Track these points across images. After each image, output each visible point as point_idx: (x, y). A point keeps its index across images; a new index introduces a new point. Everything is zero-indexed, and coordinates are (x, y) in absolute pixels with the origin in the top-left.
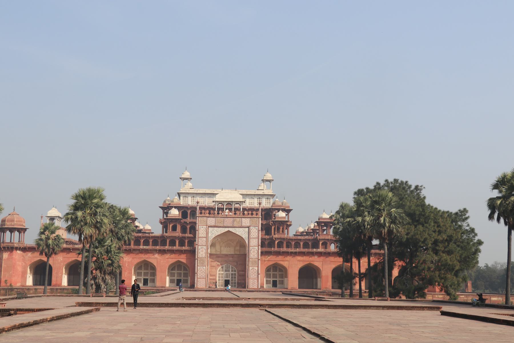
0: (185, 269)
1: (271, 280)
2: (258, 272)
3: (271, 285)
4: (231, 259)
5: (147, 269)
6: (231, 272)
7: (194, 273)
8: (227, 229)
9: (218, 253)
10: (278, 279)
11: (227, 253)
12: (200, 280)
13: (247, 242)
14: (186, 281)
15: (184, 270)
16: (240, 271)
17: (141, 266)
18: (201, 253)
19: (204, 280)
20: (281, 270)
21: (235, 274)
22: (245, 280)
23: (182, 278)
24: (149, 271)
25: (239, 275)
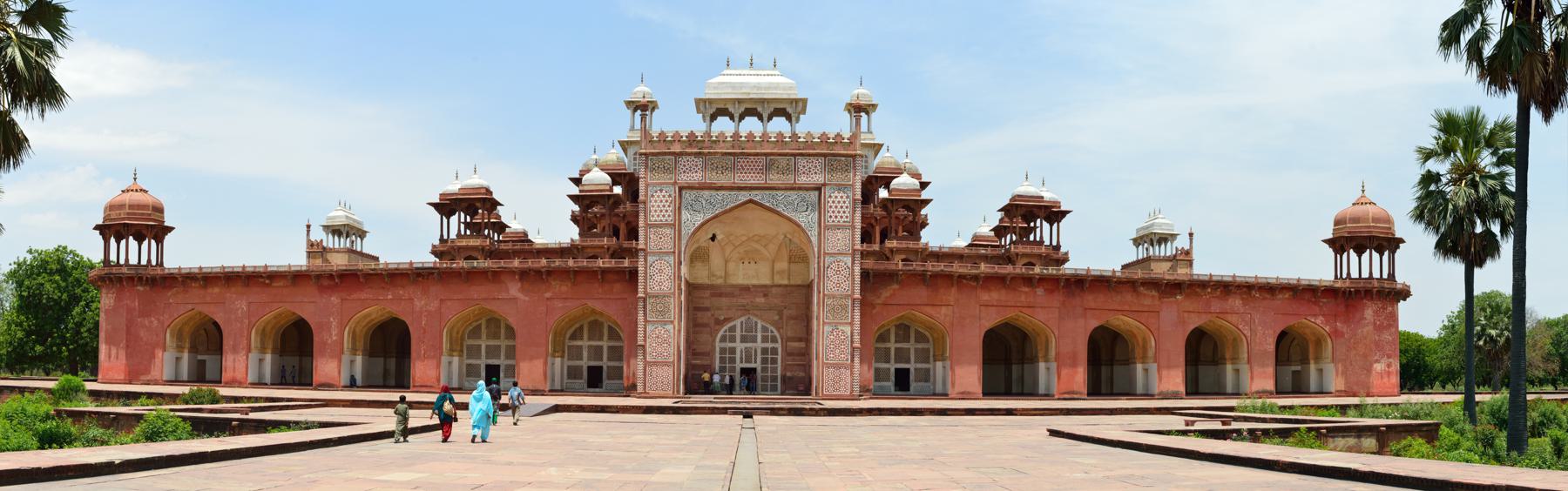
0: (614, 335)
1: (892, 366)
3: (890, 384)
4: (760, 300)
5: (496, 336)
6: (759, 345)
7: (636, 348)
8: (744, 196)
9: (720, 281)
10: (912, 366)
13: (814, 240)
15: (610, 338)
17: (479, 327)
18: (657, 278)
20: (921, 338)
21: (774, 351)
22: (807, 367)
23: (605, 363)
24: (503, 343)
25: (788, 353)
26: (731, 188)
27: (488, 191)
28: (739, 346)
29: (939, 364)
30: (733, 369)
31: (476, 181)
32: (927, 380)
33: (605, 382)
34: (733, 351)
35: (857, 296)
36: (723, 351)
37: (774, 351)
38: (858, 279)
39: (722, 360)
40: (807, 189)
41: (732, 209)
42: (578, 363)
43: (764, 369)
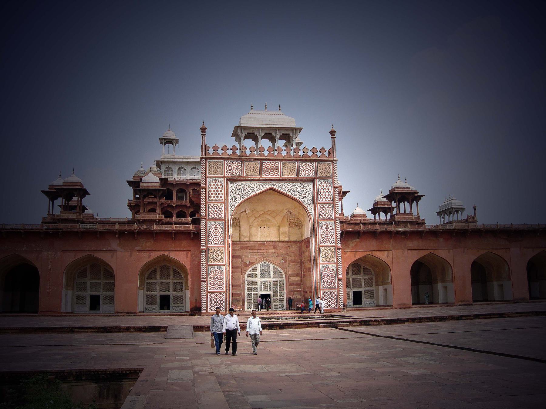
0: (177, 275)
1: (352, 290)
2: (338, 275)
3: (351, 301)
4: (272, 251)
6: (272, 279)
7: (199, 281)
8: (267, 186)
9: (246, 240)
10: (362, 289)
11: (263, 240)
12: (213, 295)
13: (311, 211)
14: (180, 300)
15: (174, 277)
16: (291, 275)
19: (222, 297)
21: (281, 283)
23: (171, 293)
25: (290, 284)
26: (259, 181)
27: (81, 185)
28: (260, 280)
29: (381, 288)
30: (256, 295)
31: (74, 179)
32: (372, 298)
33: (172, 306)
34: (255, 283)
35: (339, 246)
36: (249, 283)
37: (281, 283)
38: (339, 236)
39: (249, 289)
40: (305, 181)
41: (259, 194)
42: (153, 294)
43: (275, 295)
